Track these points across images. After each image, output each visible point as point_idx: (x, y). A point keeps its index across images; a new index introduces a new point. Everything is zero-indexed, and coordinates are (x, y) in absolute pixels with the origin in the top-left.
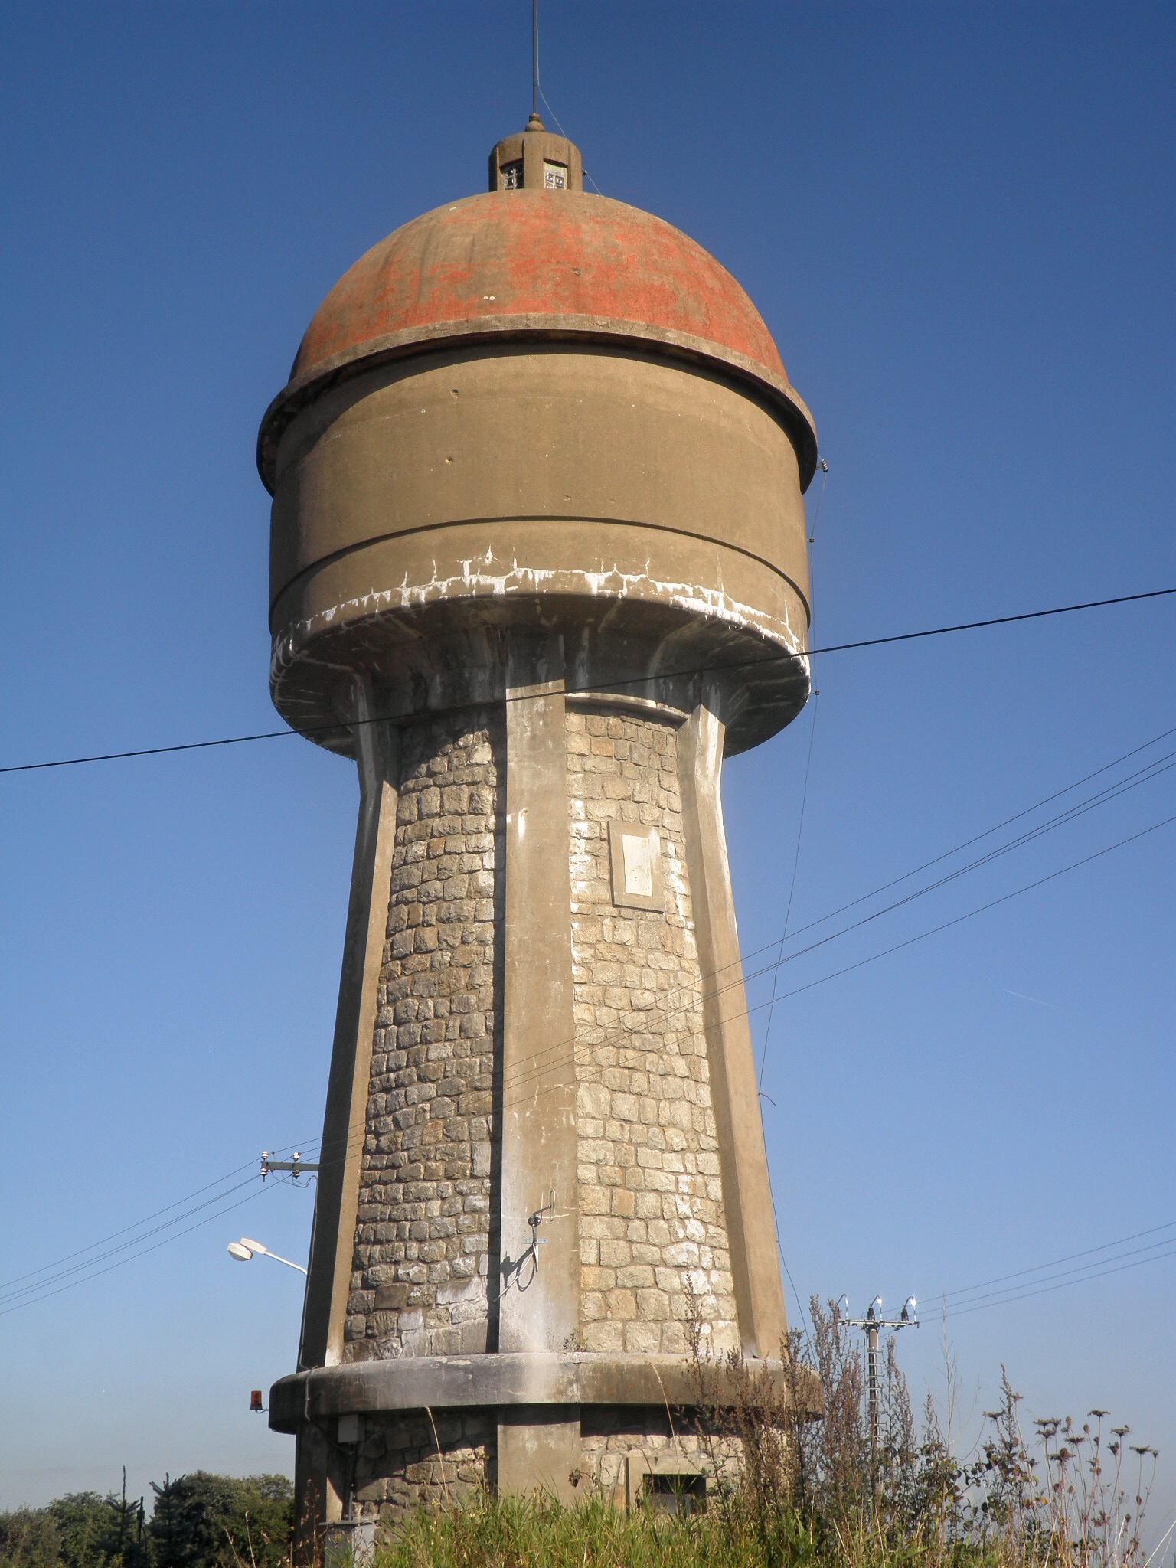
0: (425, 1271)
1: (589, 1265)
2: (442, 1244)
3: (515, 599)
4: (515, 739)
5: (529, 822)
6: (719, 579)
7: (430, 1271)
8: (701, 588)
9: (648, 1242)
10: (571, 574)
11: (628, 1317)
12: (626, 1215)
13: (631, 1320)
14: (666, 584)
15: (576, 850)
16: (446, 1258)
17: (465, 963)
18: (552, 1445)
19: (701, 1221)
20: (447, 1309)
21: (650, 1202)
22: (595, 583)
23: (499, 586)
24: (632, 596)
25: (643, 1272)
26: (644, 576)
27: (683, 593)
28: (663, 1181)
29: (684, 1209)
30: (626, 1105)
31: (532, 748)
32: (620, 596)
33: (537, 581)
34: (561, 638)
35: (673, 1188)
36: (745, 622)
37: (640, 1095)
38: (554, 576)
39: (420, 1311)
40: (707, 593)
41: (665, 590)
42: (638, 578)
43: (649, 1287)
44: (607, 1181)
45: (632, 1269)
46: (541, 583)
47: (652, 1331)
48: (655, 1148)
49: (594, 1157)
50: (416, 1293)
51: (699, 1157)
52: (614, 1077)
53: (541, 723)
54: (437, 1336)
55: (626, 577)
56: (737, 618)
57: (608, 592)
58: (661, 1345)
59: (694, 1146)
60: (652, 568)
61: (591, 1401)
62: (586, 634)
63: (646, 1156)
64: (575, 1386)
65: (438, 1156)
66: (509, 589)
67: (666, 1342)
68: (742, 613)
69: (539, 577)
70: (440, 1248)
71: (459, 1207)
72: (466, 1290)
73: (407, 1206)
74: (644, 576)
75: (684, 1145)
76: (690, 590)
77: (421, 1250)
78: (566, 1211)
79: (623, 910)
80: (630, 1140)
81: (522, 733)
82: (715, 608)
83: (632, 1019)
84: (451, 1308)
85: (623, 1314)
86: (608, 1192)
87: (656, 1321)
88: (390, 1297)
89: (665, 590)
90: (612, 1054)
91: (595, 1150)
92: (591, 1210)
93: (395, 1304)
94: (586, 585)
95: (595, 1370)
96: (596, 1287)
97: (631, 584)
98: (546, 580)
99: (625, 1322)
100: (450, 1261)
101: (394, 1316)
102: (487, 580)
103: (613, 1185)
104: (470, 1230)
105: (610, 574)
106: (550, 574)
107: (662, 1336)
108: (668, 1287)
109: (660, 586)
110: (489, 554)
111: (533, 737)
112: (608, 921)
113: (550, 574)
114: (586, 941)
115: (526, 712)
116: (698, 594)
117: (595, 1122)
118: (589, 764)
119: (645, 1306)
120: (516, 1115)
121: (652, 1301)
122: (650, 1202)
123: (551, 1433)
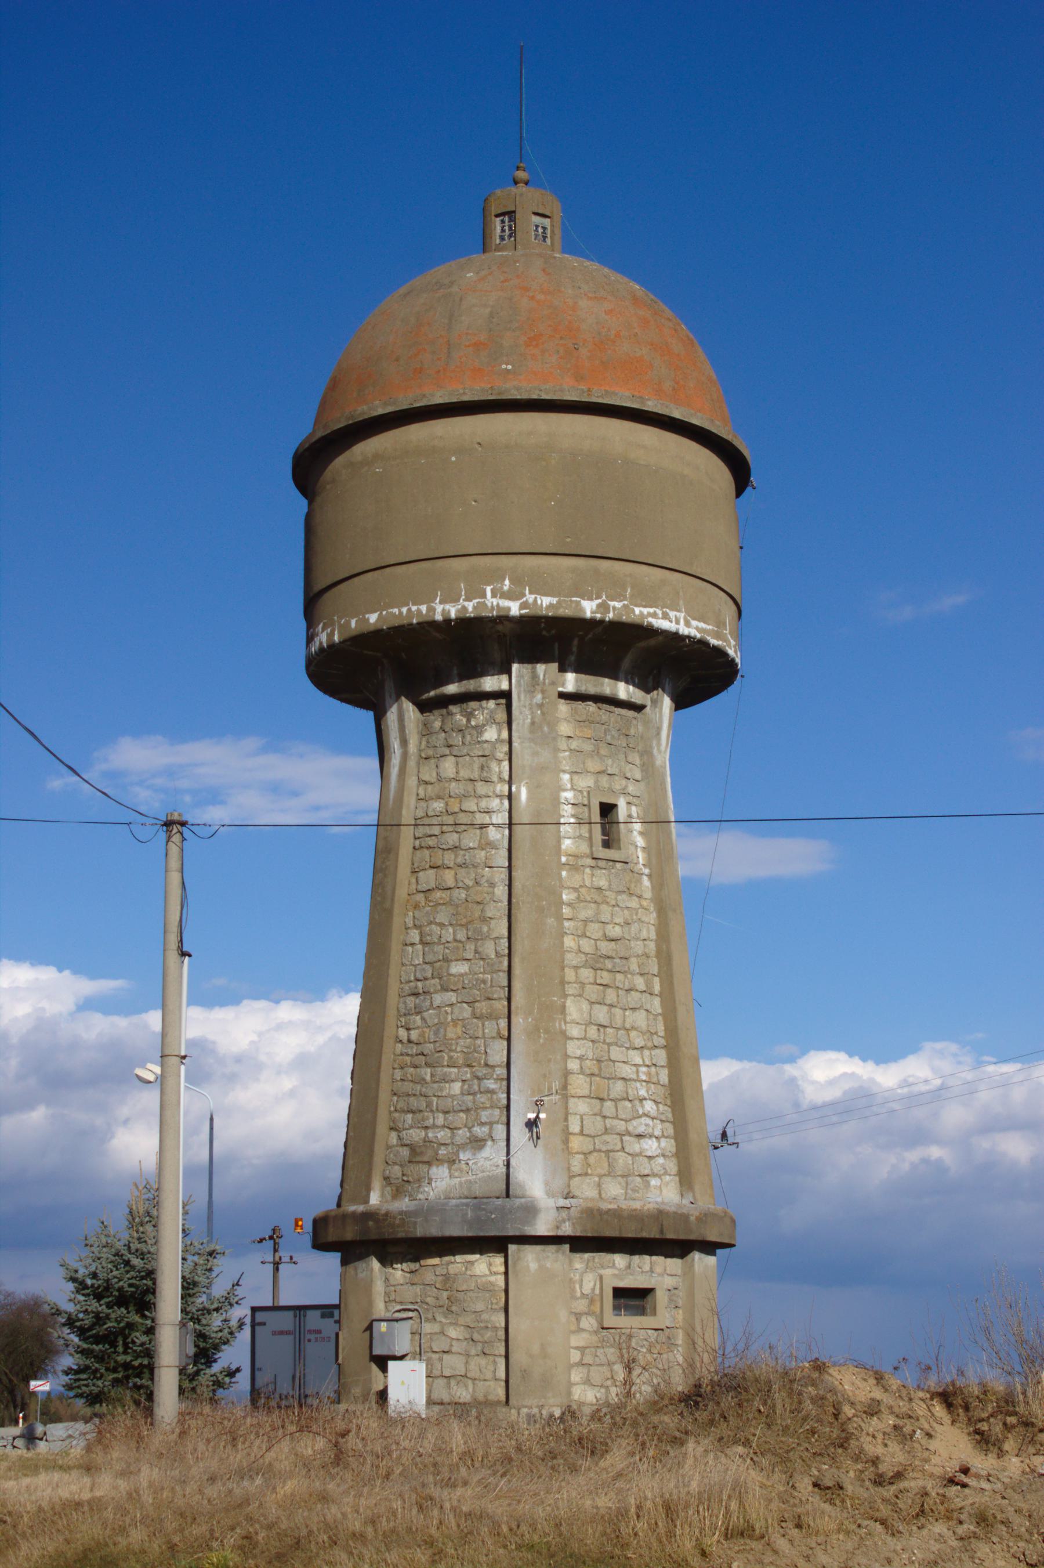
0: (449, 1135)
1: (575, 1134)
2: (463, 1115)
4: (518, 724)
5: (529, 791)
6: (681, 602)
7: (453, 1136)
8: (668, 611)
9: (616, 1118)
10: (571, 601)
11: (603, 1172)
12: (601, 1096)
13: (605, 1175)
14: (642, 609)
15: (565, 814)
16: (466, 1126)
17: (479, 900)
18: (548, 1265)
19: (654, 1101)
20: (468, 1164)
21: (618, 1087)
22: (589, 608)
23: (515, 609)
24: (616, 619)
25: (613, 1141)
26: (626, 602)
27: (654, 615)
28: (627, 1071)
29: (643, 1092)
30: (601, 1014)
31: (532, 732)
32: (607, 619)
33: (544, 606)
34: (556, 645)
35: (634, 1077)
36: (699, 636)
37: (611, 1006)
38: (558, 602)
39: (446, 1165)
40: (672, 614)
41: (641, 613)
42: (621, 604)
43: (618, 1151)
44: (588, 1072)
45: (606, 1137)
47: (620, 1184)
48: (622, 1046)
49: (578, 1053)
50: (443, 1151)
51: (653, 1052)
52: (592, 992)
53: (539, 712)
54: (460, 1183)
55: (612, 603)
56: (693, 633)
57: (598, 616)
58: (626, 1193)
59: (650, 1044)
60: (632, 596)
61: (578, 1234)
62: (576, 642)
63: (616, 1053)
64: (567, 1223)
65: (459, 1049)
66: (523, 612)
67: (630, 1191)
68: (697, 628)
69: (545, 603)
70: (461, 1118)
71: (476, 1087)
72: (483, 1151)
73: (435, 1086)
74: (626, 602)
75: (642, 1044)
76: (659, 612)
77: (445, 1119)
79: (600, 861)
80: (604, 1040)
81: (524, 720)
82: (677, 626)
83: (605, 947)
84: (470, 1163)
85: (600, 1171)
86: (588, 1080)
87: (623, 1176)
88: (422, 1153)
89: (641, 613)
90: (591, 975)
91: (579, 1048)
92: (576, 1093)
93: (425, 1159)
94: (582, 610)
95: (582, 1212)
96: (580, 1150)
97: (616, 609)
98: (551, 606)
99: (600, 1176)
100: (470, 1129)
101: (424, 1168)
102: (505, 603)
103: (592, 1075)
104: (485, 1105)
105: (600, 601)
106: (555, 601)
107: (627, 1187)
108: (631, 1152)
109: (637, 610)
110: (507, 582)
111: (533, 723)
112: (588, 870)
113: (555, 601)
114: (572, 886)
115: (527, 704)
116: (666, 616)
117: (580, 1026)
118: (574, 744)
119: (615, 1164)
120: (521, 1020)
121: (621, 1161)
122: (618, 1087)
123: (548, 1257)
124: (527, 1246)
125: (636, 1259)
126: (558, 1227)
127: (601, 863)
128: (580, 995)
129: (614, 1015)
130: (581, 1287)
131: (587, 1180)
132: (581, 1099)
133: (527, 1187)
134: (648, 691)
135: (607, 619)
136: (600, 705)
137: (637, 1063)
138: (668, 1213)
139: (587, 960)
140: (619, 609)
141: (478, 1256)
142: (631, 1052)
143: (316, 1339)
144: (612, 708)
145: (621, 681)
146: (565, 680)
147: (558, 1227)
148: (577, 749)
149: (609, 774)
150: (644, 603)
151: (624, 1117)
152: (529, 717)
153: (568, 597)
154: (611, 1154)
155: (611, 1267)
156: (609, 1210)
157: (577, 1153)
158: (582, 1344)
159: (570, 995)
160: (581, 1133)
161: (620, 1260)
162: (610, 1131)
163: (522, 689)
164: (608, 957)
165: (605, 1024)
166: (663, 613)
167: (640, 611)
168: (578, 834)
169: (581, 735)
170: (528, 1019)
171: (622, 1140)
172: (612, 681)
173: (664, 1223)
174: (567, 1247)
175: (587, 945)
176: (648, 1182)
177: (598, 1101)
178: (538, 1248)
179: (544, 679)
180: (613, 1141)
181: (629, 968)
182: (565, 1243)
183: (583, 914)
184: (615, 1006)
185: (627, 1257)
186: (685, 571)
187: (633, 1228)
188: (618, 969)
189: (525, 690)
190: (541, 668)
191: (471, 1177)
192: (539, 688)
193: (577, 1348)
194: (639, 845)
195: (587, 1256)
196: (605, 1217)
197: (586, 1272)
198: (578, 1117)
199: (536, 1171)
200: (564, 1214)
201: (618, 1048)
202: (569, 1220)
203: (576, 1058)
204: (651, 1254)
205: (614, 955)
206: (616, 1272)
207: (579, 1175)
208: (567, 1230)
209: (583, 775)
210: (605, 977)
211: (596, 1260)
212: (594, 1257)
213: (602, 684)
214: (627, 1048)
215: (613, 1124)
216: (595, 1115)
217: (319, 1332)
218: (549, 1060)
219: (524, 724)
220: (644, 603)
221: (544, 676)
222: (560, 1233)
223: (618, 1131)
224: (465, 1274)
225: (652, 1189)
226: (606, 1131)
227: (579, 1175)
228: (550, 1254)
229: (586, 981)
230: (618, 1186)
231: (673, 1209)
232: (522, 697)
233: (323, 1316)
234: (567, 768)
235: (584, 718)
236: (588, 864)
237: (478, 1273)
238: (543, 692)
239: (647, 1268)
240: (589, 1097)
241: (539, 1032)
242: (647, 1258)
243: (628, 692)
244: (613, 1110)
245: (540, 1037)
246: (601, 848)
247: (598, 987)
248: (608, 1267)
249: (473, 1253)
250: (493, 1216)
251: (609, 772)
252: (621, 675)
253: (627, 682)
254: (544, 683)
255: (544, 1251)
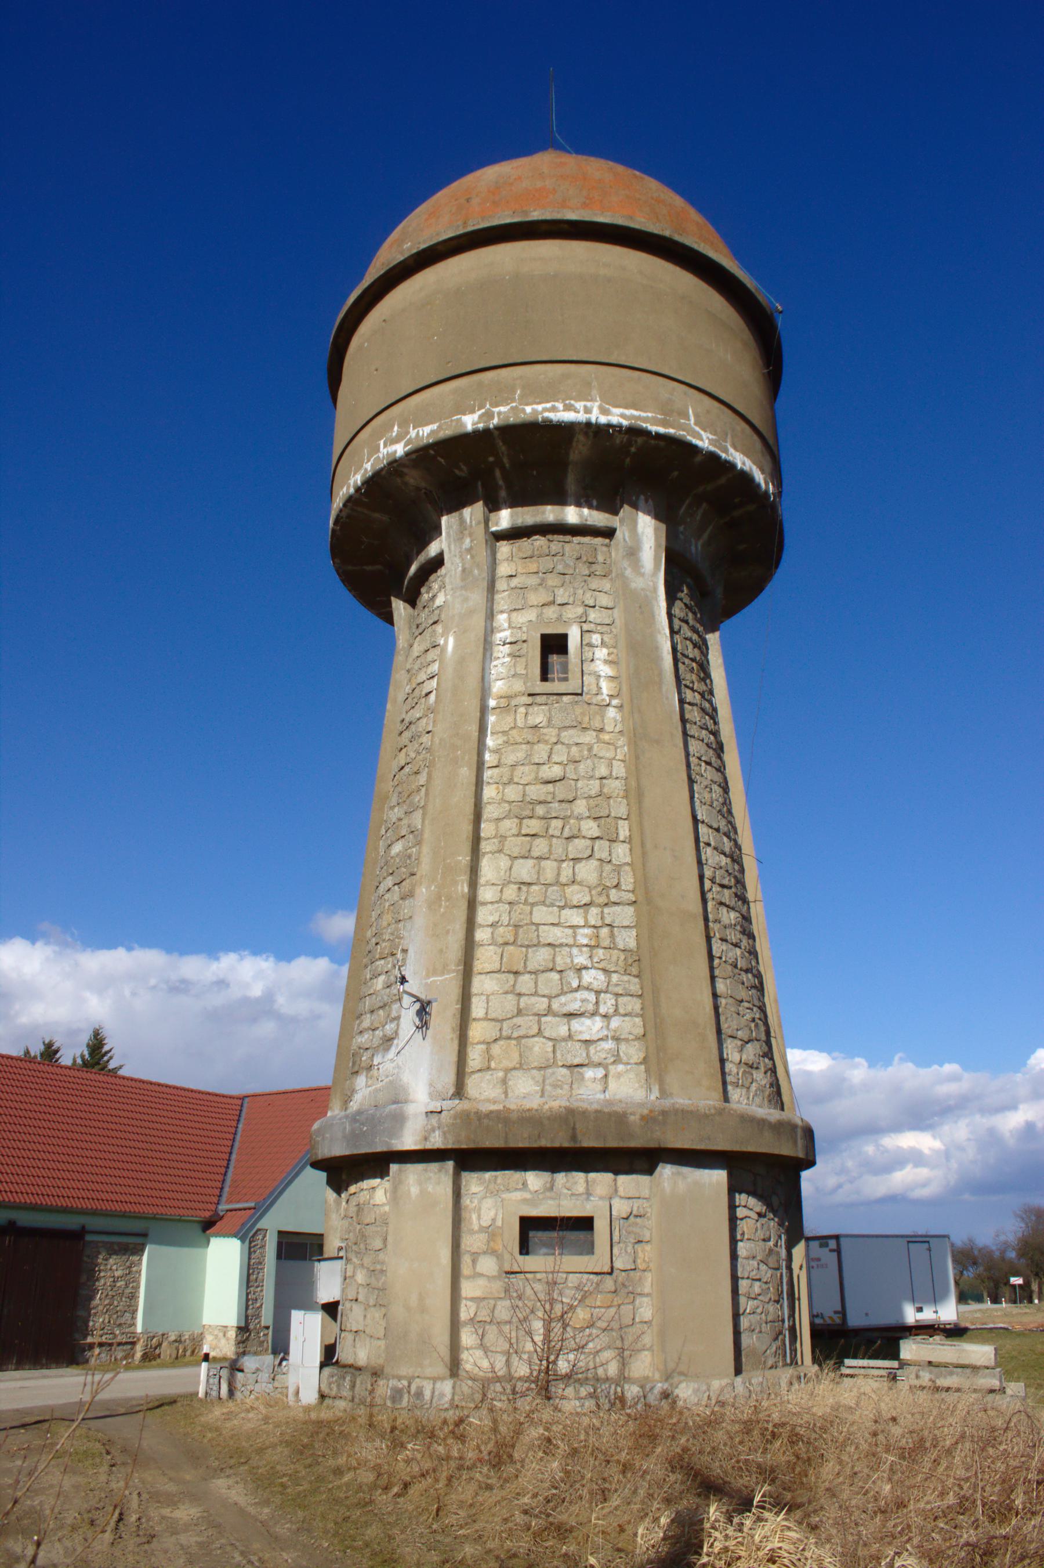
1: (479, 1020)
2: (381, 1012)
3: (414, 456)
5: (456, 641)
6: (594, 392)
8: (572, 402)
9: (536, 994)
10: (452, 421)
11: (511, 1065)
12: (515, 969)
13: (515, 1069)
14: (535, 406)
15: (500, 655)
18: (430, 1189)
19: (604, 970)
21: (540, 957)
22: (470, 422)
24: (502, 423)
25: (527, 1024)
26: (514, 404)
27: (554, 409)
28: (557, 935)
29: (581, 960)
30: (524, 870)
31: (463, 579)
32: (491, 426)
33: (425, 434)
34: (480, 483)
35: (571, 941)
36: (625, 423)
37: (540, 858)
38: (438, 427)
40: (580, 405)
41: (534, 411)
42: (508, 407)
43: (533, 1036)
44: (501, 941)
45: (518, 1020)
46: (429, 435)
47: (533, 1078)
48: (552, 905)
49: (491, 919)
51: (606, 910)
52: (514, 845)
55: (496, 410)
56: (615, 420)
57: (481, 426)
58: (543, 1091)
59: (603, 900)
60: (521, 397)
61: (450, 1146)
62: (498, 473)
63: (540, 914)
64: (437, 1133)
66: (407, 448)
67: (548, 1088)
68: (622, 416)
69: (426, 433)
74: (514, 404)
75: (586, 899)
76: (560, 406)
78: (454, 971)
79: (538, 697)
80: (526, 900)
81: (455, 570)
82: (588, 416)
83: (536, 792)
85: (507, 1064)
87: (540, 1068)
89: (534, 411)
90: (514, 825)
91: (491, 914)
94: (463, 425)
95: (455, 1117)
97: (501, 414)
98: (432, 432)
99: (507, 1071)
102: (391, 449)
103: (506, 944)
105: (483, 411)
106: (435, 426)
107: (544, 1081)
108: (554, 1035)
109: (528, 409)
110: (396, 428)
111: (464, 570)
112: (522, 710)
113: (435, 426)
114: (501, 730)
115: (457, 551)
116: (568, 408)
117: (495, 887)
118: (514, 582)
120: (424, 890)
121: (536, 1049)
122: (540, 957)
123: (430, 1178)
124: (409, 1166)
125: (561, 1177)
126: (426, 1139)
127: (539, 699)
128: (500, 851)
129: (544, 869)
130: (479, 1218)
131: (487, 1075)
132: (488, 976)
133: (411, 1090)
134: (615, 512)
135: (491, 426)
136: (550, 537)
137: (575, 923)
138: (584, 1113)
139: (510, 810)
140: (505, 412)
141: (378, 1180)
142: (566, 912)
143: (818, 1266)
144: (568, 538)
145: (570, 505)
146: (499, 518)
147: (426, 1139)
148: (519, 586)
149: (559, 605)
150: (538, 400)
151: (546, 992)
152: (460, 565)
153: (447, 418)
154: (523, 1041)
155: (520, 1190)
156: (491, 1112)
157: (478, 1043)
158: (478, 1293)
159: (488, 853)
160: (486, 1019)
161: (535, 1180)
162: (524, 1012)
163: (452, 539)
164: (540, 802)
165: (529, 880)
166: (565, 405)
167: (533, 409)
168: (513, 673)
169: (524, 571)
170: (430, 887)
171: (539, 1022)
172: (557, 508)
173: (577, 1126)
174: (450, 1165)
175: (512, 793)
176: (582, 1075)
177: (512, 976)
178: (420, 1167)
179: (471, 522)
180: (527, 1024)
181: (572, 812)
182: (449, 1160)
183: (510, 758)
184: (548, 858)
185: (546, 1176)
186: (598, 360)
187: (526, 1135)
188: (554, 815)
189: (454, 540)
190: (467, 512)
192: (466, 532)
193: (472, 1299)
194: (602, 674)
195: (488, 1175)
196: (486, 1121)
197: (485, 1197)
198: (484, 998)
199: (422, 1070)
200: (434, 1120)
201: (545, 909)
202: (439, 1128)
203: (488, 926)
204: (586, 1169)
205: (549, 799)
206: (528, 1196)
207: (480, 1070)
208: (437, 1142)
209: (523, 611)
210: (533, 826)
211: (499, 1181)
212: (496, 1177)
213: (544, 513)
214: (562, 908)
215: (529, 1002)
216: (506, 993)
217: (819, 1260)
218: (448, 932)
219: (456, 573)
220: (538, 400)
221: (471, 518)
222: (429, 1146)
223: (535, 1010)
224: (369, 1203)
225: (589, 1083)
226: (519, 1012)
227: (480, 1070)
228: (432, 1175)
229: (509, 833)
230: (531, 1082)
231: (595, 1106)
232: (453, 547)
233: (821, 1246)
234: (506, 607)
235: (529, 554)
236: (522, 703)
237: (378, 1202)
238: (470, 535)
239: (581, 1188)
240: (499, 971)
241: (440, 899)
242: (580, 1176)
243: (581, 516)
244: (532, 985)
245: (440, 906)
246: (539, 683)
247: (523, 838)
248: (516, 1189)
249: (375, 1177)
250: (365, 1128)
251: (559, 602)
252: (569, 500)
253: (578, 505)
254: (471, 526)
255: (426, 1170)
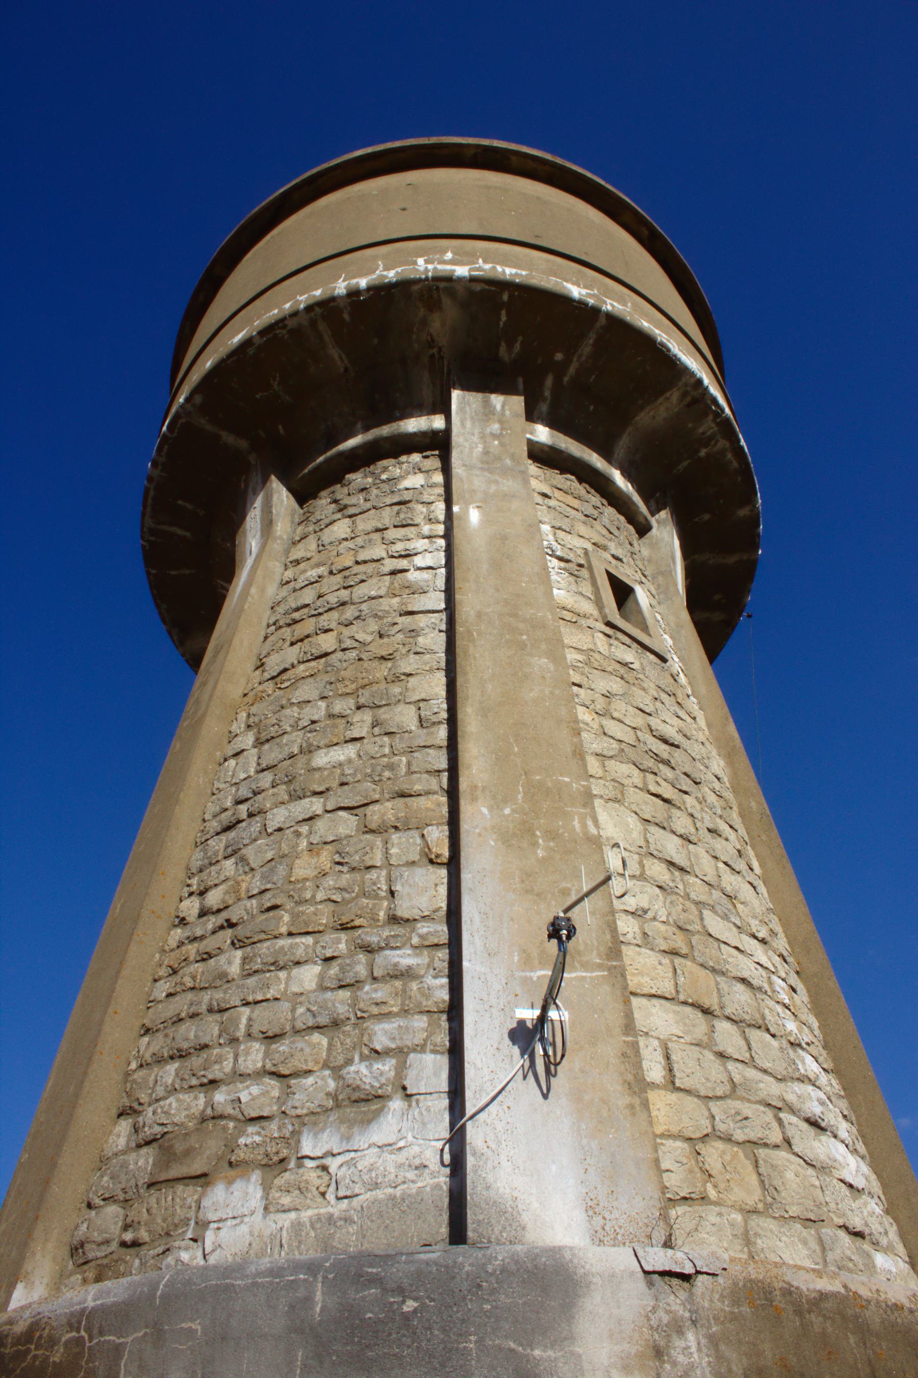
0: (276, 1093)
3: (478, 287)
4: (462, 452)
7: (288, 1092)
12: (706, 1003)
16: (326, 1066)
17: (384, 653)
20: (325, 1168)
23: (462, 271)
39: (256, 1176)
46: (511, 275)
50: (252, 1136)
53: (496, 442)
54: (297, 1227)
62: (549, 382)
64: (691, 1336)
65: (320, 896)
70: (313, 1046)
71: (361, 970)
72: (374, 1126)
73: (251, 981)
77: (267, 1054)
78: (600, 967)
81: (471, 448)
84: (333, 1164)
86: (666, 961)
88: (188, 1152)
92: (640, 985)
93: (197, 1167)
96: (675, 1129)
100: (337, 1071)
101: (188, 1193)
104: (385, 1009)
119: (777, 1182)
120: (485, 810)
131: (711, 1215)
133: (526, 1218)
156: (823, 1296)
160: (671, 1084)
163: (468, 416)
190: (497, 400)
191: (338, 1209)
226: (734, 1089)
241: (534, 834)
245: (535, 844)
250: (410, 1305)
